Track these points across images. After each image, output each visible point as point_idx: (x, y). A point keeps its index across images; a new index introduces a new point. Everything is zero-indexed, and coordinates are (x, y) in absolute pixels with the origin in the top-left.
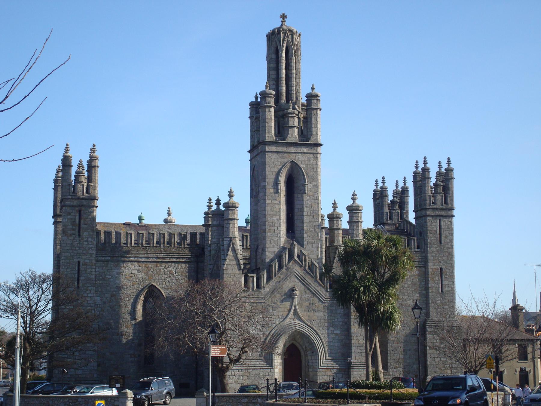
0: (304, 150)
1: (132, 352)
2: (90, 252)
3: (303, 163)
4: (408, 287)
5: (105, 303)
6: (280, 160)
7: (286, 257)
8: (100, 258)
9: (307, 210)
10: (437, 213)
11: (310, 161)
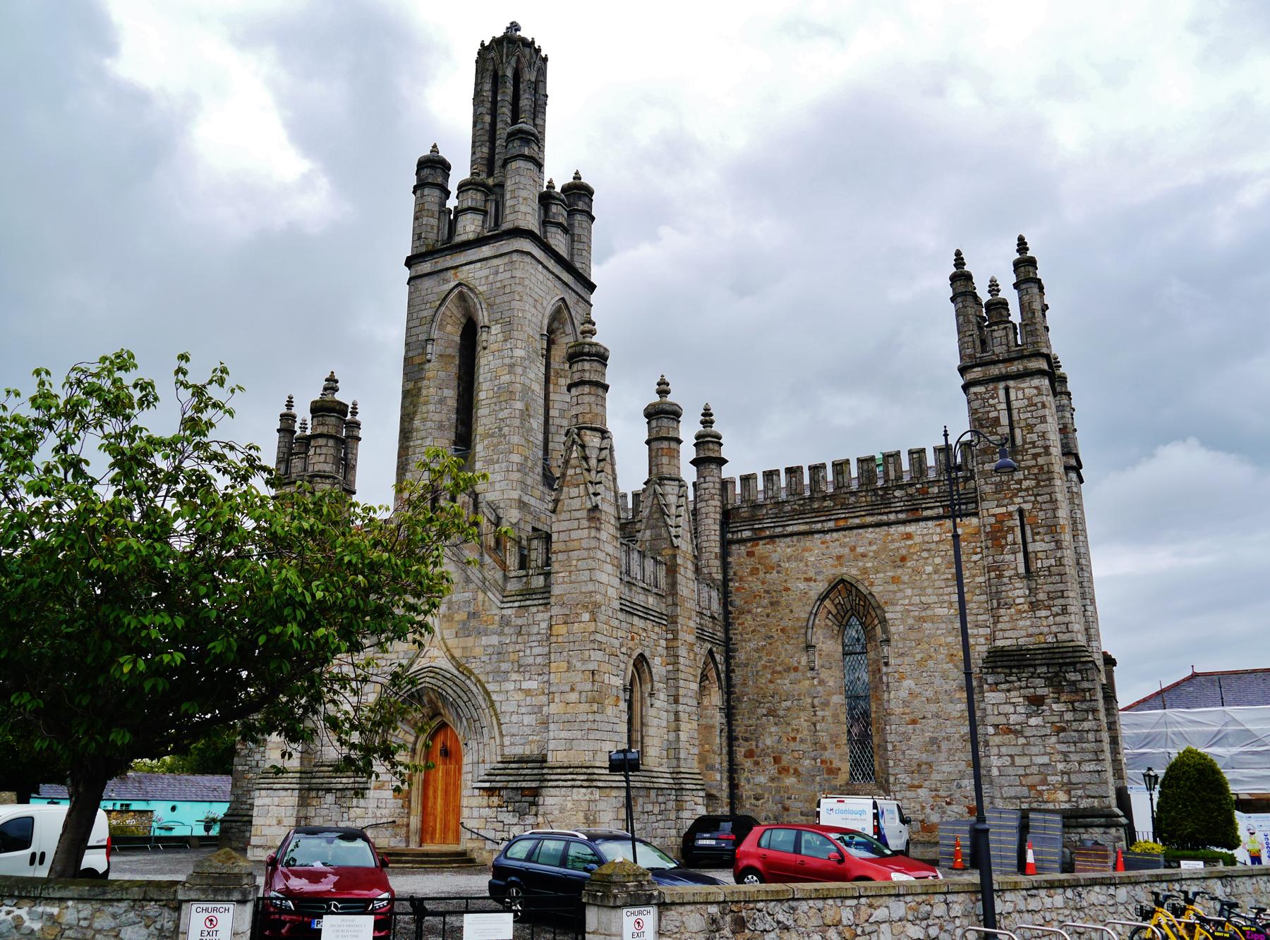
4: (936, 572)
10: (994, 371)
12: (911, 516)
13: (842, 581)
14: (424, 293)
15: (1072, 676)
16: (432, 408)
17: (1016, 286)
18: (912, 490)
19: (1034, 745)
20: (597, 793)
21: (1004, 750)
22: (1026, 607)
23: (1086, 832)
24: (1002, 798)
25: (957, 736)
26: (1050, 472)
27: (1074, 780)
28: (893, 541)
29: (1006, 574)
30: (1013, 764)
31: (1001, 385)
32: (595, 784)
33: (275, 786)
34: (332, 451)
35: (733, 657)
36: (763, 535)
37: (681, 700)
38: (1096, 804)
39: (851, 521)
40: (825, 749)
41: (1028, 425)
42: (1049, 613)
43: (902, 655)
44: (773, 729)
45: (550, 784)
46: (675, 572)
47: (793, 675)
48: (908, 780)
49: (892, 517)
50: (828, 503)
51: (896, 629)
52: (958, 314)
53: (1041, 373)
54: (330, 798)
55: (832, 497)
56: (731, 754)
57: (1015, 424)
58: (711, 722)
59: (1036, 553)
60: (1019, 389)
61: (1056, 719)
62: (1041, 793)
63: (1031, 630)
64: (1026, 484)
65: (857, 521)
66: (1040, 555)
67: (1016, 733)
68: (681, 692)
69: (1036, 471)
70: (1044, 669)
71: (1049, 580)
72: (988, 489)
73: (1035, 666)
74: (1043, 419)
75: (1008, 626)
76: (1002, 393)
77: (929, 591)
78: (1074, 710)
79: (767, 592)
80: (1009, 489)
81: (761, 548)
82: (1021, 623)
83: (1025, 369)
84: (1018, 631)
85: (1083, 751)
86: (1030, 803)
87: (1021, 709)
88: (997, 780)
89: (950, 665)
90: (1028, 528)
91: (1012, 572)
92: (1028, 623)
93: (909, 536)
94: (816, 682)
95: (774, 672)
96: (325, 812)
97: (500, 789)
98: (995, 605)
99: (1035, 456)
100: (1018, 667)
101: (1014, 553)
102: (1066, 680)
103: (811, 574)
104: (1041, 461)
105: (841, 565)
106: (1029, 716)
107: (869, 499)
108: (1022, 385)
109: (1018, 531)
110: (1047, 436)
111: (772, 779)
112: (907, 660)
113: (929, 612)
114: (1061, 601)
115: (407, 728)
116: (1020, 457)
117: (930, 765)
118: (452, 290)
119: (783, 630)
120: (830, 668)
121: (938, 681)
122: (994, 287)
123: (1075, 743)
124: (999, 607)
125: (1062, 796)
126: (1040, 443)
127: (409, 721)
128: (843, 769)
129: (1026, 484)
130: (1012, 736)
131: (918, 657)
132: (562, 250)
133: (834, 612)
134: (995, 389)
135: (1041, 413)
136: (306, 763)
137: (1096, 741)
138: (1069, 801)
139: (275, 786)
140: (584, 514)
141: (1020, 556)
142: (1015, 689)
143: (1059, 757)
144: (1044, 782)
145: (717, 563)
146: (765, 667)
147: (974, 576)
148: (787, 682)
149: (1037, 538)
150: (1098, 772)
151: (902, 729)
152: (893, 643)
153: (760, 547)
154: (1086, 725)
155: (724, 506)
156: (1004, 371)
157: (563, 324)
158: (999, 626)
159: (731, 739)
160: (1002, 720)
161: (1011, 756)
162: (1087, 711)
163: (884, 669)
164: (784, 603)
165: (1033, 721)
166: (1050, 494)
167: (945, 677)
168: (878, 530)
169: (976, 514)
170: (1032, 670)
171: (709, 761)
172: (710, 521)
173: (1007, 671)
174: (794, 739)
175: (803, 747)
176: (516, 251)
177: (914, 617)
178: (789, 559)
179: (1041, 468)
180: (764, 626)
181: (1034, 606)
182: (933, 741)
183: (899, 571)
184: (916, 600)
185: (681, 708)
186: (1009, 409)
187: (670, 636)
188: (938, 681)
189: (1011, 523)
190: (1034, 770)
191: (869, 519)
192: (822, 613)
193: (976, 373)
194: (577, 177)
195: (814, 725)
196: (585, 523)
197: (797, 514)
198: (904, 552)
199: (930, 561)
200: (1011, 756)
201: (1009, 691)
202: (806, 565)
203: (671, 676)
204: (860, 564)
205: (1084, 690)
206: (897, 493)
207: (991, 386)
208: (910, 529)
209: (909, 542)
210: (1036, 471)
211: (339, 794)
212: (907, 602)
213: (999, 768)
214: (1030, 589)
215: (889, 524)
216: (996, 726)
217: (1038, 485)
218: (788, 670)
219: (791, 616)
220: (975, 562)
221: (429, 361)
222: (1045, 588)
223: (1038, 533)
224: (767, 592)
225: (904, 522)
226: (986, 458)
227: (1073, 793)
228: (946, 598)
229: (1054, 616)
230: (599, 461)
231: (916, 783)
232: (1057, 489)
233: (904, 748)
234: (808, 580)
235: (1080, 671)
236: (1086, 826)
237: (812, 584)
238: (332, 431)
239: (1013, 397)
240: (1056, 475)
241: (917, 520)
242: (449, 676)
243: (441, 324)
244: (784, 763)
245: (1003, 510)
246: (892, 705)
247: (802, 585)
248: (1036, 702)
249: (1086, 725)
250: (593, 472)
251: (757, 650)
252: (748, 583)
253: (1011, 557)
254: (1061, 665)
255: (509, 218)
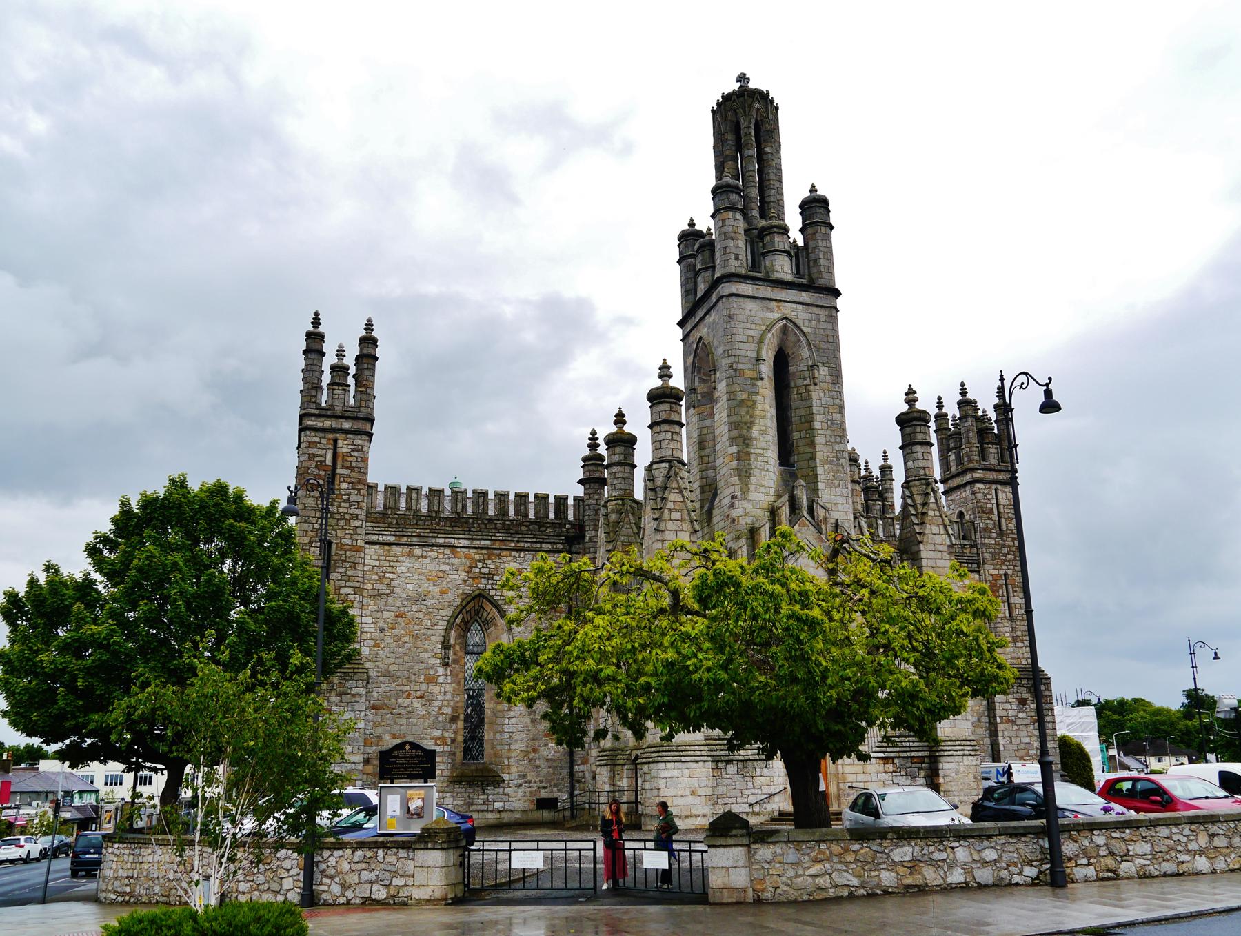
0: (805, 296)
1: (438, 733)
2: (357, 523)
3: (807, 323)
5: (382, 630)
6: (760, 314)
7: (785, 512)
8: (374, 538)
9: (819, 418)
10: (991, 476)
11: (819, 321)
14: (748, 313)
21: (1006, 733)
31: (994, 487)
33: (683, 759)
54: (732, 769)
64: (1009, 557)
67: (1013, 722)
96: (727, 782)
97: (893, 758)
129: (1009, 557)
139: (683, 759)
140: (945, 548)
160: (1004, 713)
165: (1021, 715)
186: (998, 505)
196: (947, 556)
211: (740, 765)
239: (1000, 496)
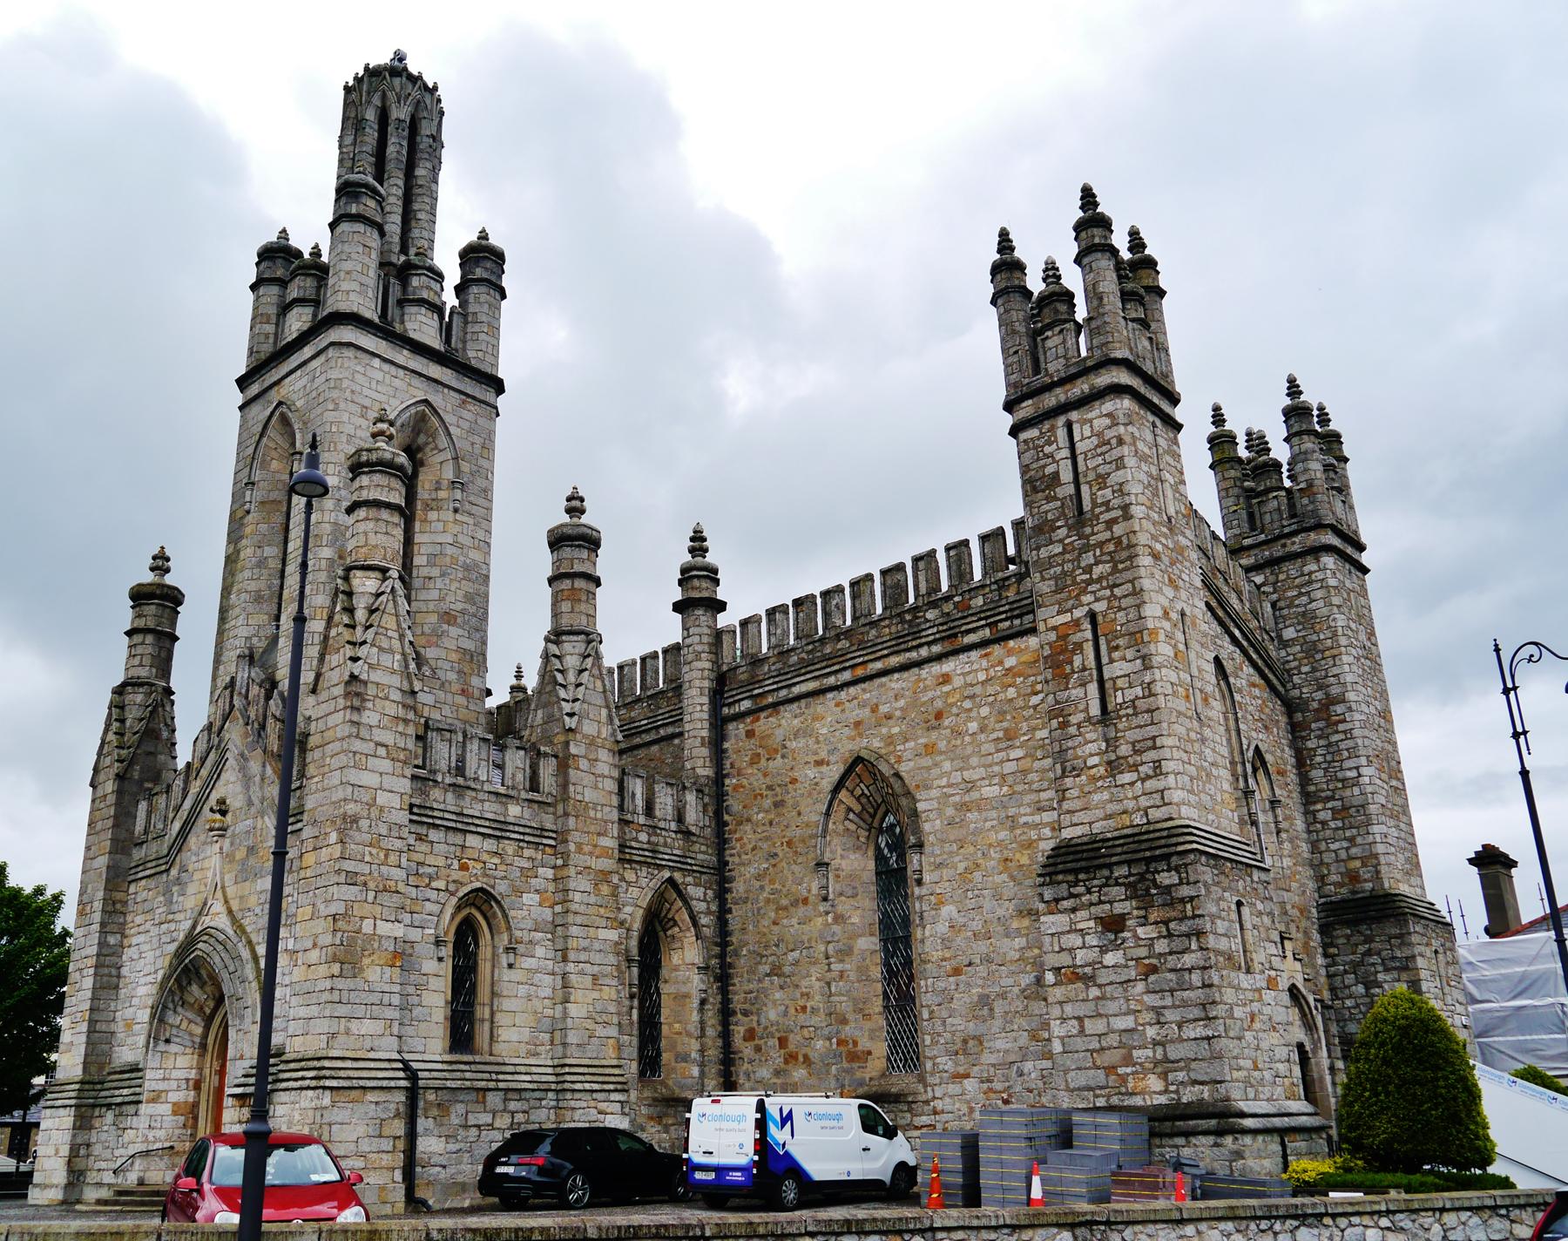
4: (982, 730)
10: (1050, 400)
12: (948, 647)
13: (859, 760)
15: (1166, 878)
16: (247, 574)
17: (1078, 261)
18: (948, 607)
19: (1113, 999)
20: (327, 1099)
21: (1068, 1009)
22: (1102, 770)
23: (1188, 1144)
24: (1068, 1089)
25: (1016, 990)
26: (1130, 546)
27: (1172, 1055)
28: (926, 689)
29: (1074, 719)
30: (1082, 1031)
31: (1061, 421)
32: (322, 1083)
34: (149, 650)
35: (729, 890)
36: (765, 702)
37: (572, 955)
38: (1206, 1095)
39: (871, 666)
40: (844, 1021)
41: (1099, 476)
42: (1134, 776)
43: (939, 866)
44: (778, 995)
45: (284, 1085)
46: (568, 766)
47: (801, 910)
48: (950, 1066)
49: (924, 652)
50: (844, 644)
51: (931, 827)
52: (1002, 323)
53: (1117, 390)
55: (848, 633)
56: (726, 1035)
57: (1082, 479)
58: (684, 989)
59: (1113, 680)
60: (1084, 422)
61: (1143, 952)
62: (1123, 1079)
63: (1111, 808)
64: (1098, 571)
65: (879, 665)
66: (1120, 683)
67: (1089, 980)
68: (572, 943)
69: (1111, 547)
70: (1124, 870)
71: (1135, 721)
72: (1045, 587)
73: (1110, 866)
74: (1120, 463)
75: (1076, 804)
76: (1061, 433)
77: (974, 761)
78: (1170, 935)
79: (770, 788)
80: (1074, 583)
81: (764, 724)
82: (1096, 797)
83: (1092, 387)
84: (1095, 813)
85: (1185, 1004)
86: (1109, 1097)
87: (1092, 940)
88: (1059, 1060)
89: (1005, 877)
90: (1102, 641)
91: (1081, 716)
92: (1106, 796)
93: (946, 679)
94: (830, 918)
95: (780, 908)
98: (1059, 772)
99: (1110, 523)
100: (1086, 870)
101: (1084, 685)
102: (1156, 886)
103: (823, 755)
104: (1118, 530)
105: (860, 735)
106: (1103, 950)
107: (893, 629)
108: (1090, 416)
109: (1089, 649)
110: (1126, 488)
111: (777, 1073)
112: (946, 873)
113: (975, 795)
114: (1152, 755)
115: (190, 1015)
116: (1088, 530)
117: (979, 1040)
118: (272, 413)
119: (789, 843)
120: (854, 896)
121: (988, 904)
122: (1051, 272)
123: (1172, 991)
124: (1064, 775)
125: (1155, 1083)
126: (1115, 502)
127: (192, 1005)
128: (876, 1053)
129: (1098, 571)
130: (1080, 985)
131: (961, 867)
132: (433, 340)
133: (857, 808)
134: (1053, 429)
135: (1116, 453)
136: (93, 1069)
137: (1204, 986)
138: (1166, 1091)
141: (1093, 688)
142: (1082, 907)
143: (1148, 1016)
144: (1128, 1060)
145: (705, 752)
146: (768, 901)
147: (1034, 729)
148: (794, 921)
149: (1116, 655)
150: (1208, 1038)
151: (941, 985)
152: (927, 849)
153: (762, 721)
154: (1188, 960)
155: (716, 663)
156: (1062, 398)
157: (434, 436)
158: (1066, 806)
159: (726, 1013)
160: (1065, 959)
161: (1080, 1019)
162: (1188, 936)
163: (917, 891)
164: (790, 802)
165: (1110, 958)
166: (1132, 581)
167: (998, 897)
168: (905, 675)
169: (1033, 631)
170: (1106, 872)
171: (679, 1048)
172: (694, 692)
173: (1071, 878)
174: (804, 1008)
175: (815, 1020)
176: (332, 344)
177: (955, 805)
178: (796, 736)
179: (1118, 541)
180: (767, 839)
181: (1113, 767)
182: (984, 1001)
183: (934, 735)
184: (957, 777)
185: (571, 967)
186: (1074, 457)
187: (560, 862)
188: (988, 904)
189: (1077, 638)
190: (1113, 1040)
191: (894, 661)
192: (838, 813)
193: (1027, 409)
194: (483, 235)
195: (829, 984)
197: (805, 667)
198: (939, 704)
199: (974, 714)
200: (1080, 1019)
201: (1074, 910)
202: (813, 740)
203: (559, 921)
204: (884, 730)
205: (1182, 900)
206: (930, 615)
207: (1047, 426)
208: (948, 666)
209: (946, 688)
210: (1111, 547)
212: (944, 782)
213: (1062, 1038)
214: (1107, 741)
215: (919, 664)
216: (1057, 970)
217: (1115, 570)
218: (795, 903)
219: (799, 821)
220: (1035, 707)
221: (248, 512)
222: (1129, 733)
223: (1117, 648)
224: (770, 788)
225: (939, 658)
226: (1042, 539)
227: (1171, 1076)
228: (996, 769)
229: (1143, 780)
230: (372, 612)
231: (961, 1070)
232: (1142, 572)
233: (945, 1014)
234: (819, 763)
235: (1177, 869)
236: (1188, 1134)
237: (824, 769)
238: (151, 624)
240: (1140, 550)
241: (955, 652)
242: (222, 937)
243: (263, 461)
244: (792, 1047)
245: (1066, 618)
246: (928, 947)
247: (811, 773)
248: (1113, 925)
249: (1188, 960)
250: (359, 629)
251: (758, 877)
252: (746, 778)
253: (1079, 692)
254: (1148, 861)
255: (329, 302)
